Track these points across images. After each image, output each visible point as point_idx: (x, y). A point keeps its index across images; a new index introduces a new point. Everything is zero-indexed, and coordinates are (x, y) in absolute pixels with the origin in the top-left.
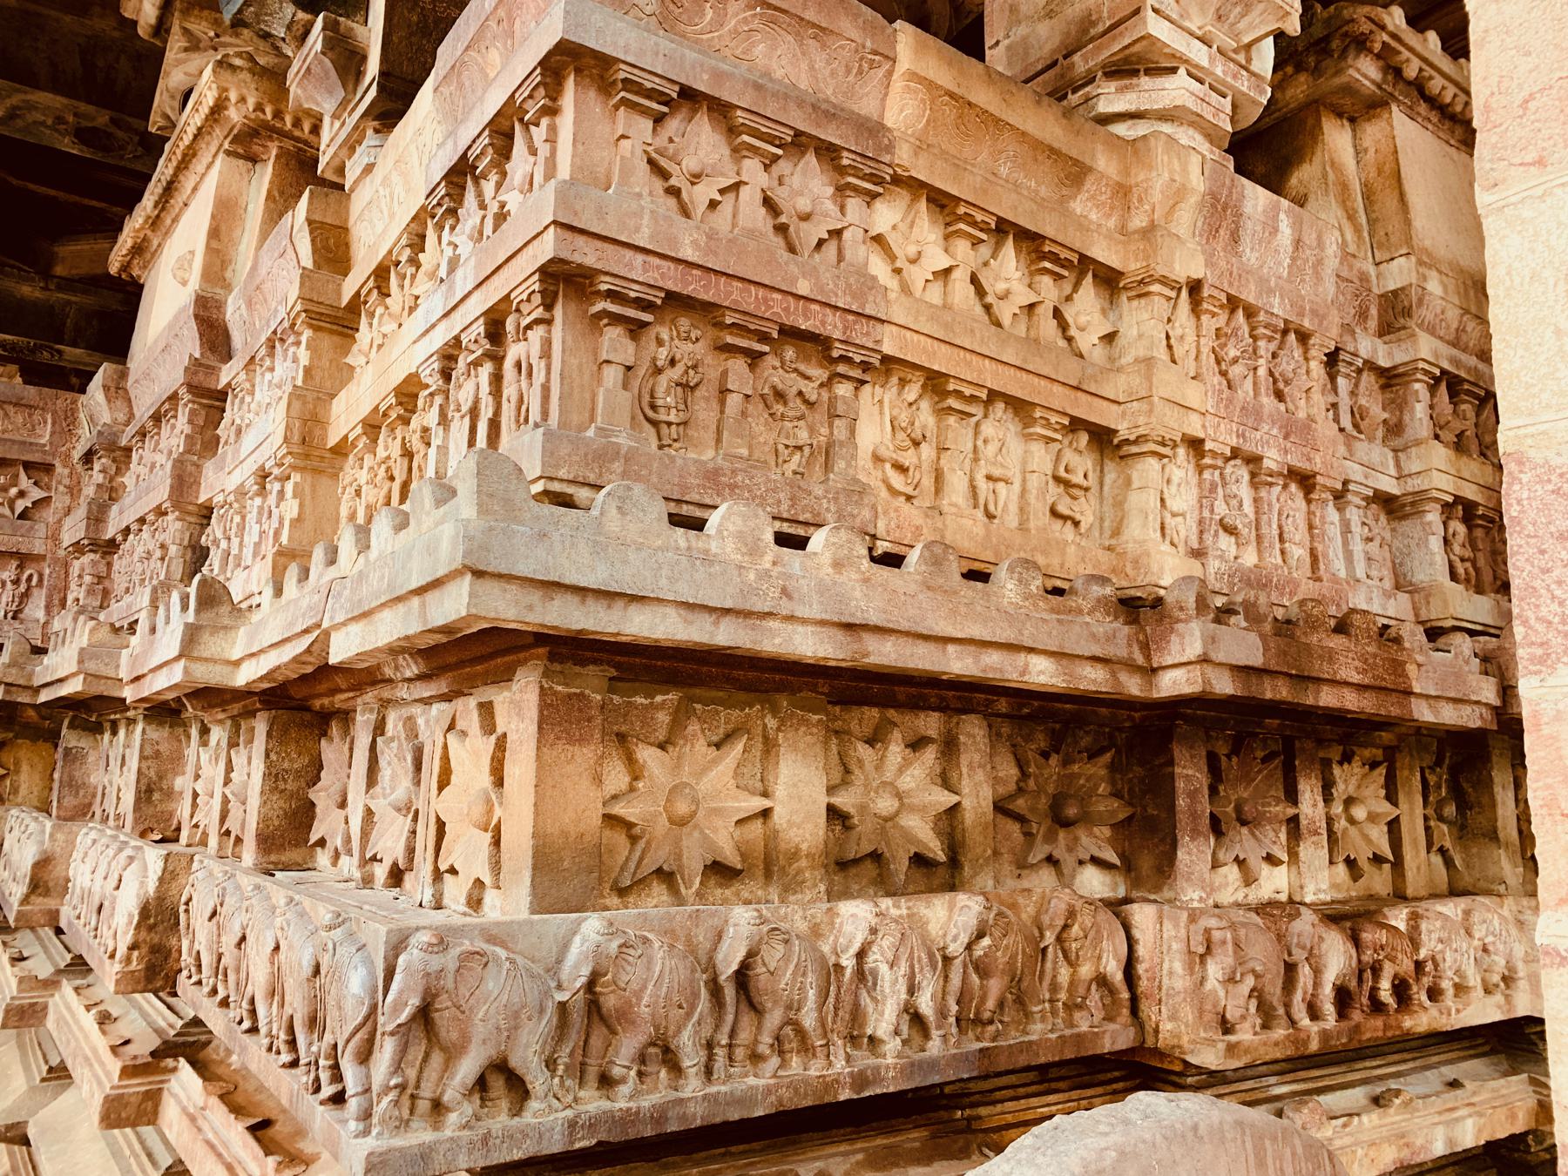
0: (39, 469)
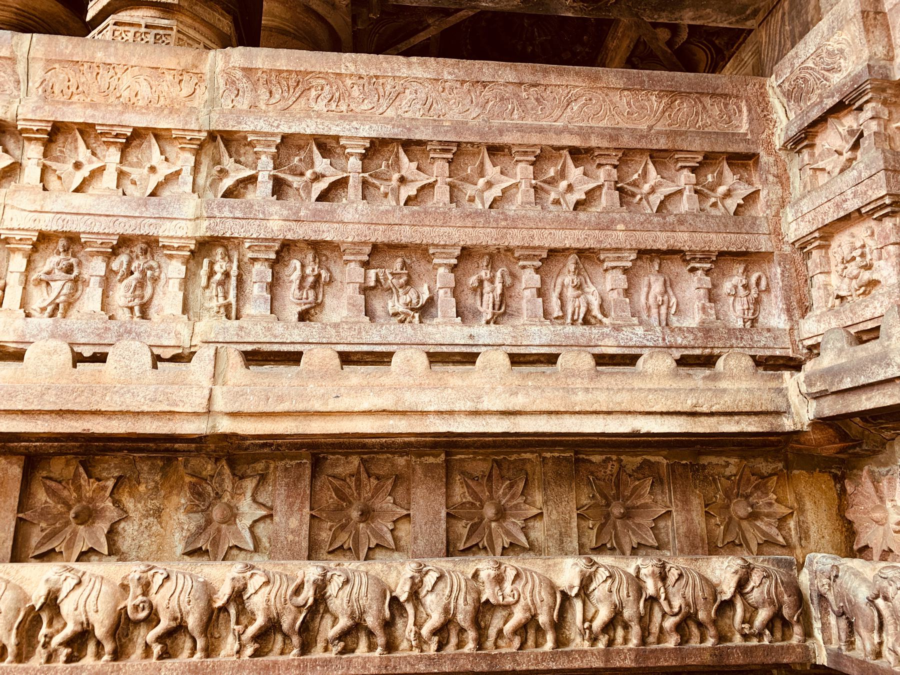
0: (743, 161)
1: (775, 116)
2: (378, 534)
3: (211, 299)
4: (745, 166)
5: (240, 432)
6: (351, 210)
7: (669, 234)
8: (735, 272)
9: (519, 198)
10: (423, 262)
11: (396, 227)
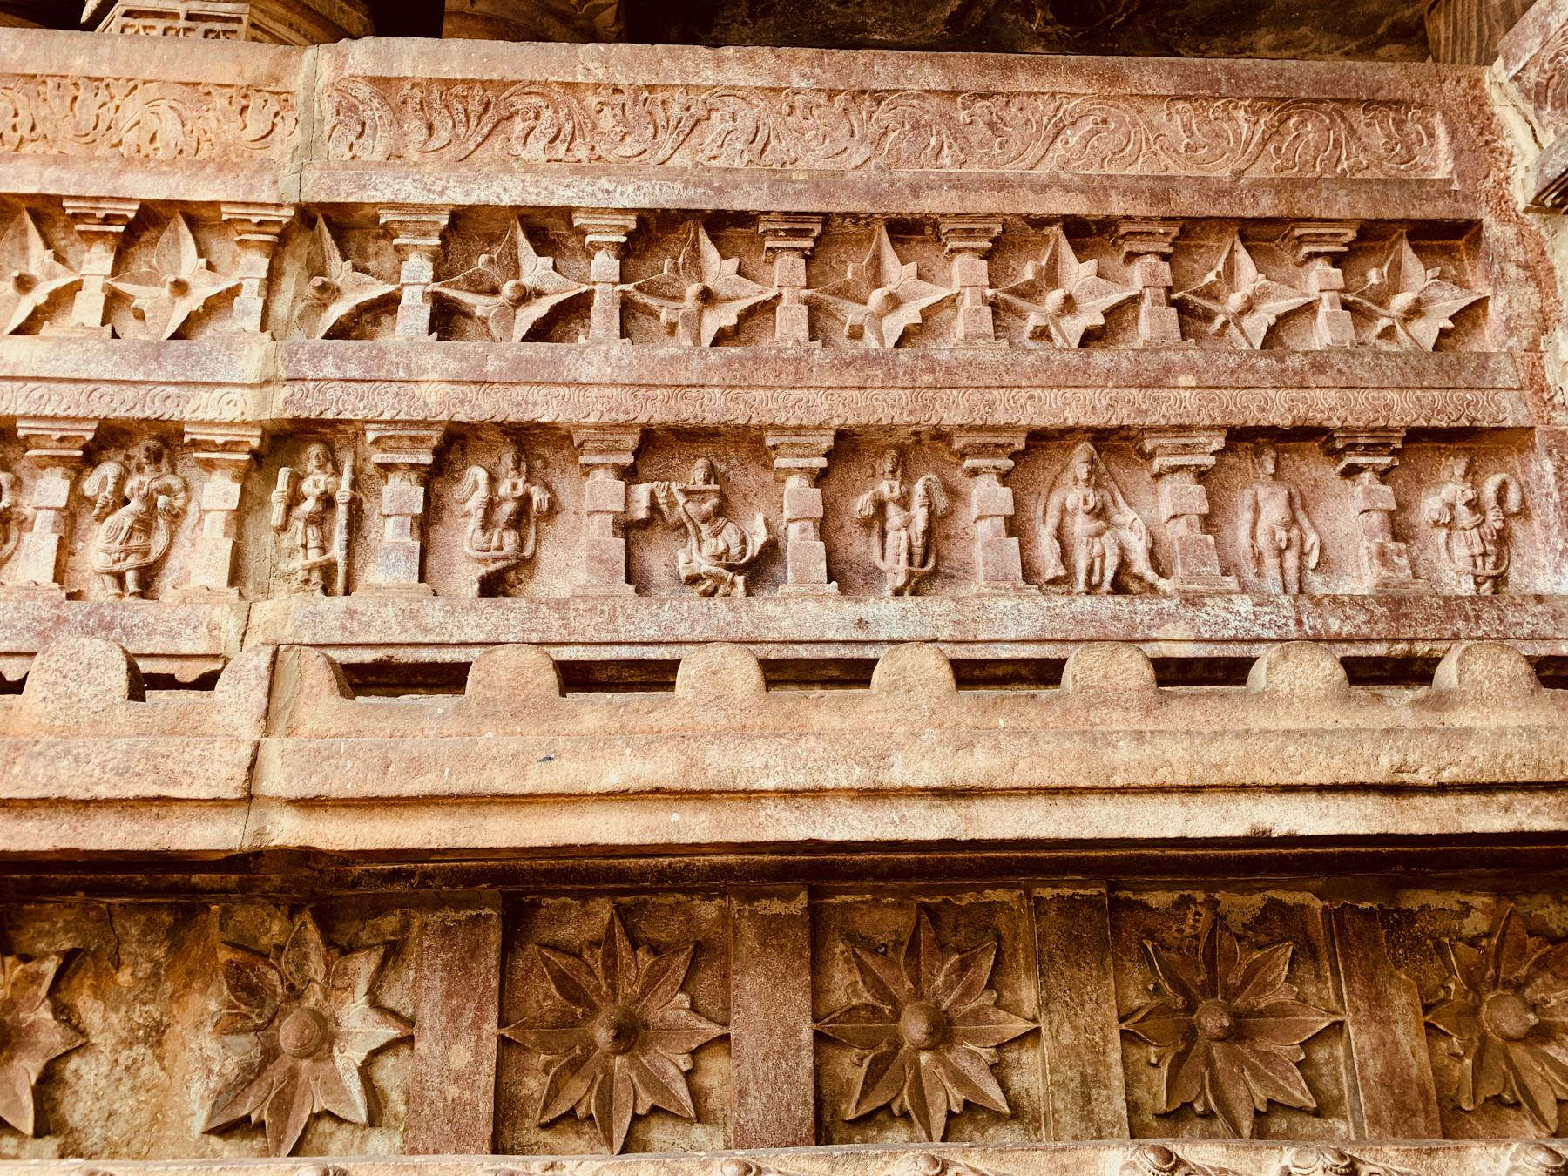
0: (1446, 238)
1: (1508, 143)
2: (654, 1083)
3: (292, 553)
4: (1448, 252)
5: (321, 845)
6: (595, 358)
7: (1294, 393)
8: (1445, 475)
9: (960, 327)
10: (753, 468)
11: (693, 392)
